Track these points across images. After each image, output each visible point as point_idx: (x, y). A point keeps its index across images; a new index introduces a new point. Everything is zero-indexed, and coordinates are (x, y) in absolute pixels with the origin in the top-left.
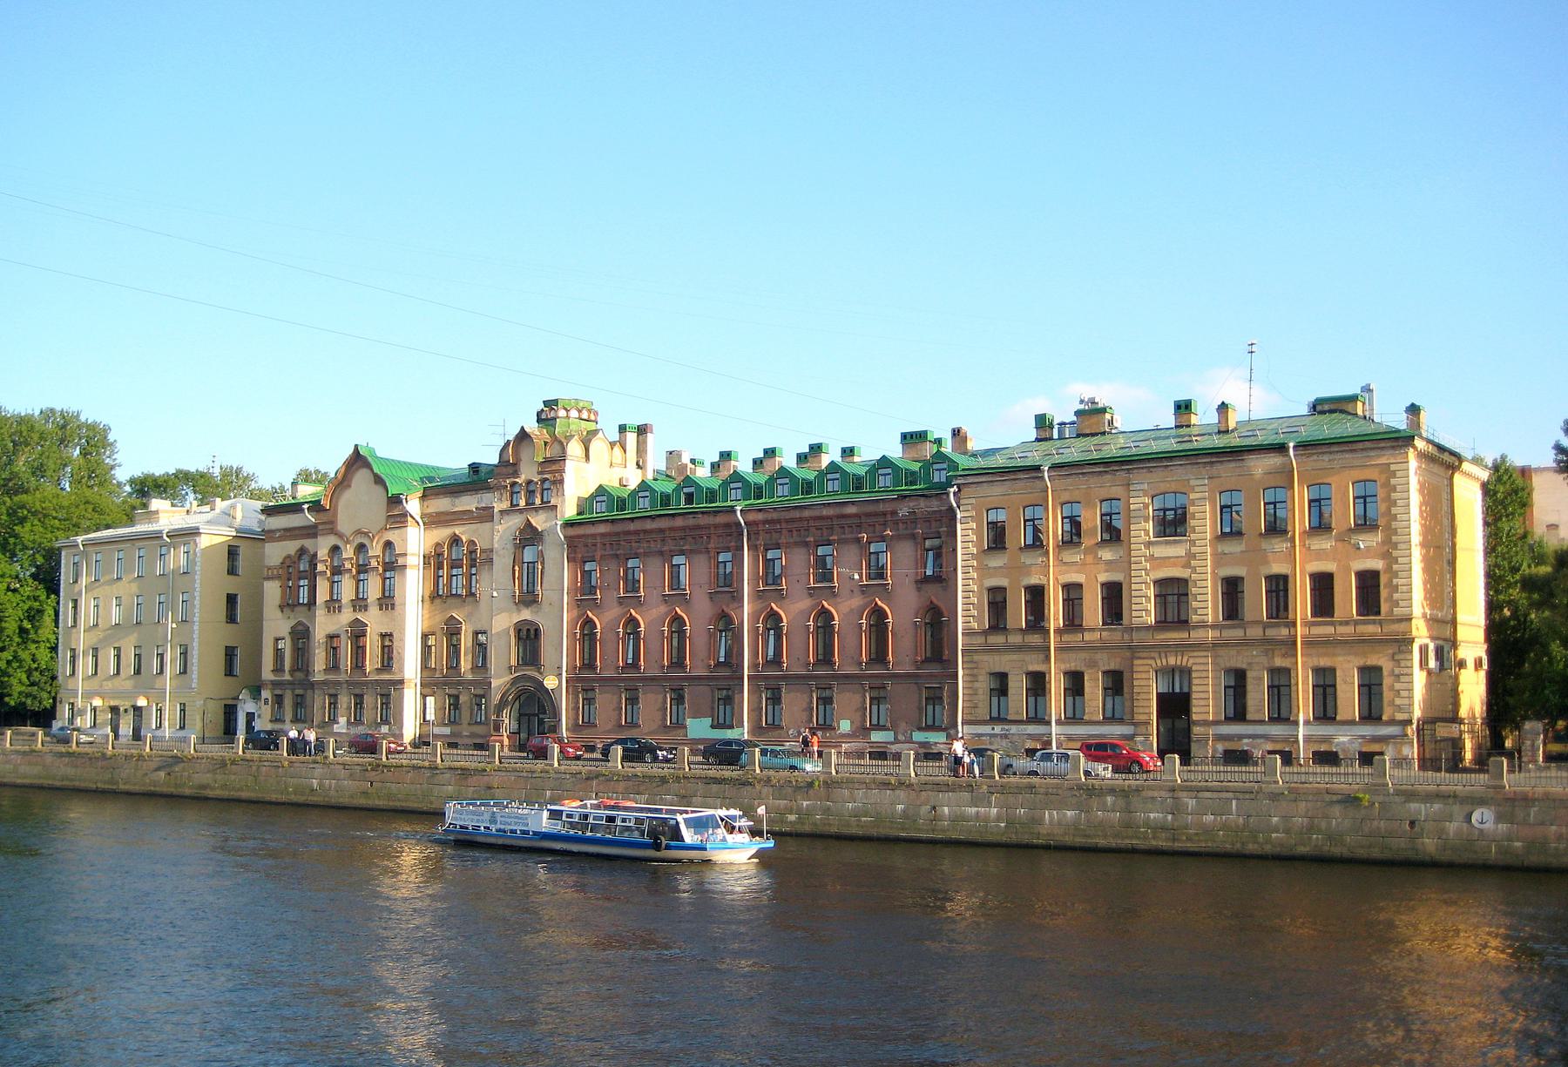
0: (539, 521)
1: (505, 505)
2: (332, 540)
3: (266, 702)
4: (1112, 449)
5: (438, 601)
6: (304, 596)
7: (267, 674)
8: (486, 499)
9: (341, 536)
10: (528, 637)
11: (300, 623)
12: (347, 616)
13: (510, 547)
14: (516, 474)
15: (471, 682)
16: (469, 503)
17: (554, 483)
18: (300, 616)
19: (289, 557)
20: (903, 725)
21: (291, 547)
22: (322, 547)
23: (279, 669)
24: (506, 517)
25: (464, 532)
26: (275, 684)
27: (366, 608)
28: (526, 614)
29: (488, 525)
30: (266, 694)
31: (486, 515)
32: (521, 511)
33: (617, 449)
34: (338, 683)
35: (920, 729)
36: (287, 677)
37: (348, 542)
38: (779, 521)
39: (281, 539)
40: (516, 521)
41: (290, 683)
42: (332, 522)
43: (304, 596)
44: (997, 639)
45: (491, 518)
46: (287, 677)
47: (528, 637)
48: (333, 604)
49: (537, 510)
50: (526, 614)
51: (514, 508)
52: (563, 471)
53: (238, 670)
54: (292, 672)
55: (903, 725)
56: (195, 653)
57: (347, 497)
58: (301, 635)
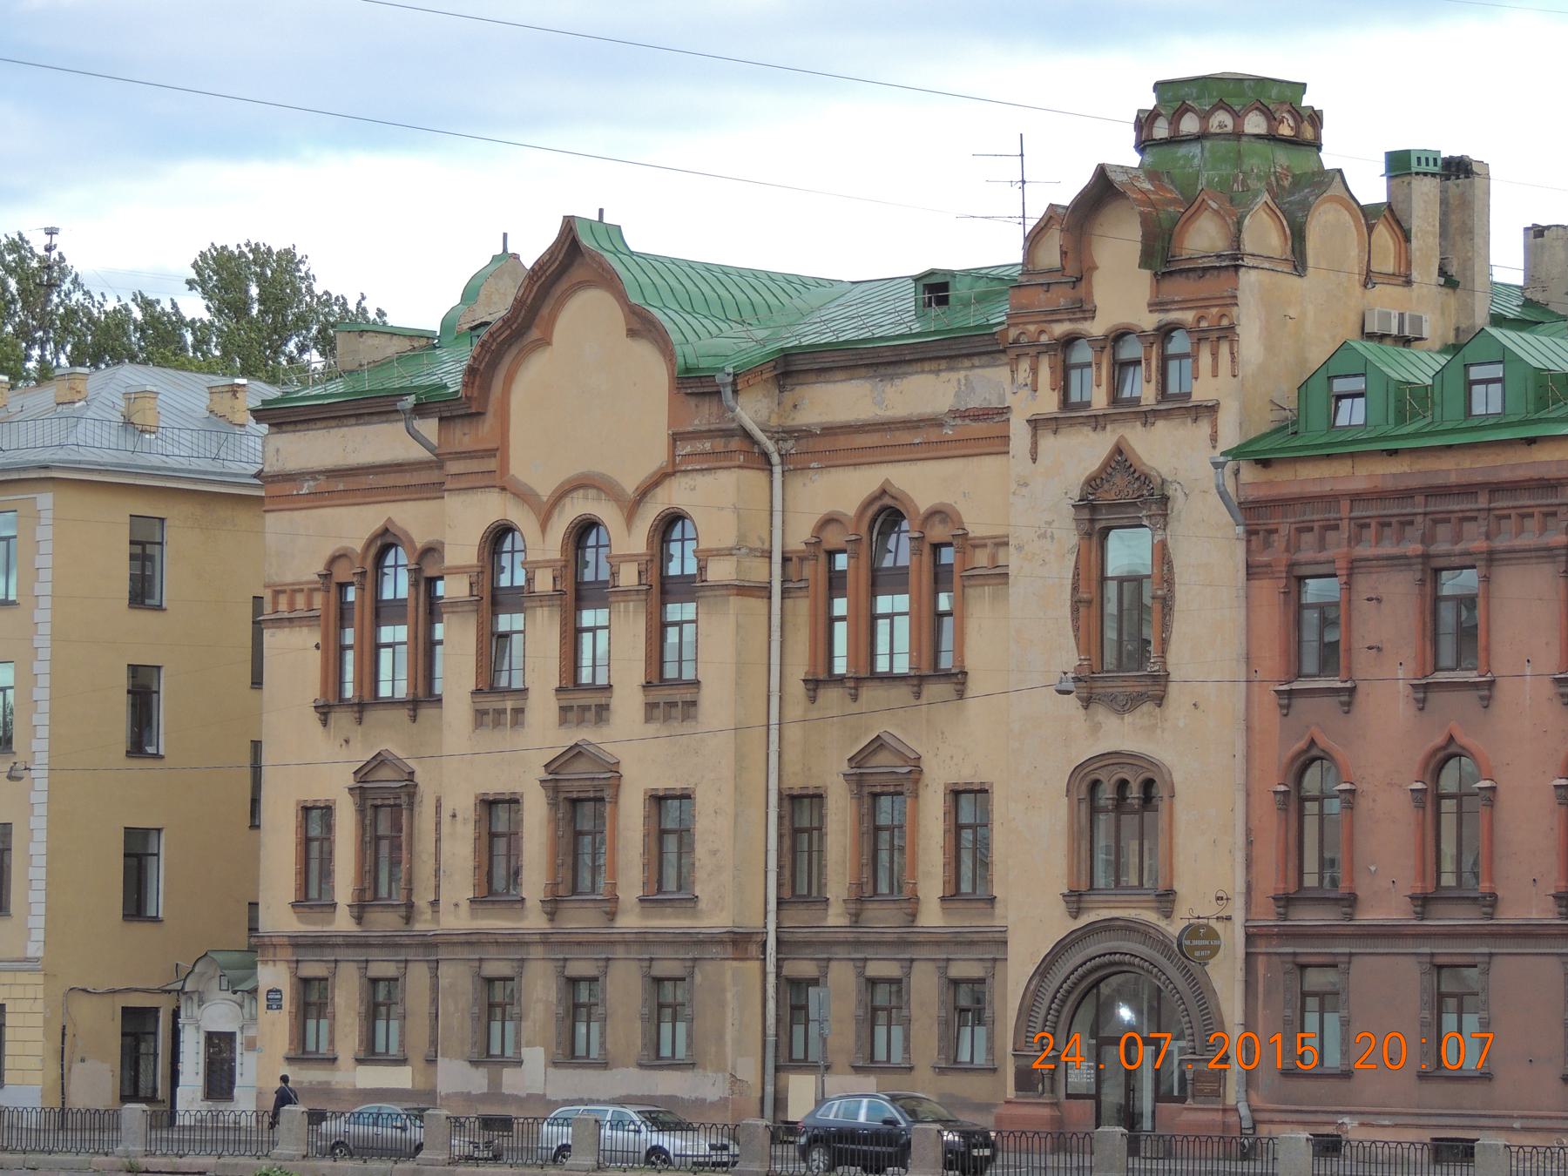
0: (1166, 450)
3: (274, 1001)
5: (832, 697)
6: (393, 679)
7: (278, 917)
8: (990, 383)
9: (523, 495)
10: (1122, 800)
11: (380, 760)
12: (543, 733)
13: (1068, 536)
14: (1083, 309)
15: (938, 941)
16: (926, 393)
17: (1200, 336)
18: (387, 736)
21: (353, 526)
22: (458, 524)
23: (312, 891)
24: (1048, 442)
25: (922, 484)
26: (300, 945)
28: (1120, 734)
29: (990, 464)
30: (273, 975)
31: (982, 431)
32: (1098, 422)
33: (1384, 235)
36: (343, 922)
39: (319, 499)
40: (1084, 453)
41: (351, 943)
42: (498, 452)
43: (393, 679)
45: (1000, 444)
46: (343, 922)
47: (1122, 800)
48: (496, 699)
49: (1147, 417)
50: (1120, 734)
51: (1071, 414)
52: (1233, 301)
53: (159, 899)
56: (39, 848)
57: (533, 386)
58: (386, 802)
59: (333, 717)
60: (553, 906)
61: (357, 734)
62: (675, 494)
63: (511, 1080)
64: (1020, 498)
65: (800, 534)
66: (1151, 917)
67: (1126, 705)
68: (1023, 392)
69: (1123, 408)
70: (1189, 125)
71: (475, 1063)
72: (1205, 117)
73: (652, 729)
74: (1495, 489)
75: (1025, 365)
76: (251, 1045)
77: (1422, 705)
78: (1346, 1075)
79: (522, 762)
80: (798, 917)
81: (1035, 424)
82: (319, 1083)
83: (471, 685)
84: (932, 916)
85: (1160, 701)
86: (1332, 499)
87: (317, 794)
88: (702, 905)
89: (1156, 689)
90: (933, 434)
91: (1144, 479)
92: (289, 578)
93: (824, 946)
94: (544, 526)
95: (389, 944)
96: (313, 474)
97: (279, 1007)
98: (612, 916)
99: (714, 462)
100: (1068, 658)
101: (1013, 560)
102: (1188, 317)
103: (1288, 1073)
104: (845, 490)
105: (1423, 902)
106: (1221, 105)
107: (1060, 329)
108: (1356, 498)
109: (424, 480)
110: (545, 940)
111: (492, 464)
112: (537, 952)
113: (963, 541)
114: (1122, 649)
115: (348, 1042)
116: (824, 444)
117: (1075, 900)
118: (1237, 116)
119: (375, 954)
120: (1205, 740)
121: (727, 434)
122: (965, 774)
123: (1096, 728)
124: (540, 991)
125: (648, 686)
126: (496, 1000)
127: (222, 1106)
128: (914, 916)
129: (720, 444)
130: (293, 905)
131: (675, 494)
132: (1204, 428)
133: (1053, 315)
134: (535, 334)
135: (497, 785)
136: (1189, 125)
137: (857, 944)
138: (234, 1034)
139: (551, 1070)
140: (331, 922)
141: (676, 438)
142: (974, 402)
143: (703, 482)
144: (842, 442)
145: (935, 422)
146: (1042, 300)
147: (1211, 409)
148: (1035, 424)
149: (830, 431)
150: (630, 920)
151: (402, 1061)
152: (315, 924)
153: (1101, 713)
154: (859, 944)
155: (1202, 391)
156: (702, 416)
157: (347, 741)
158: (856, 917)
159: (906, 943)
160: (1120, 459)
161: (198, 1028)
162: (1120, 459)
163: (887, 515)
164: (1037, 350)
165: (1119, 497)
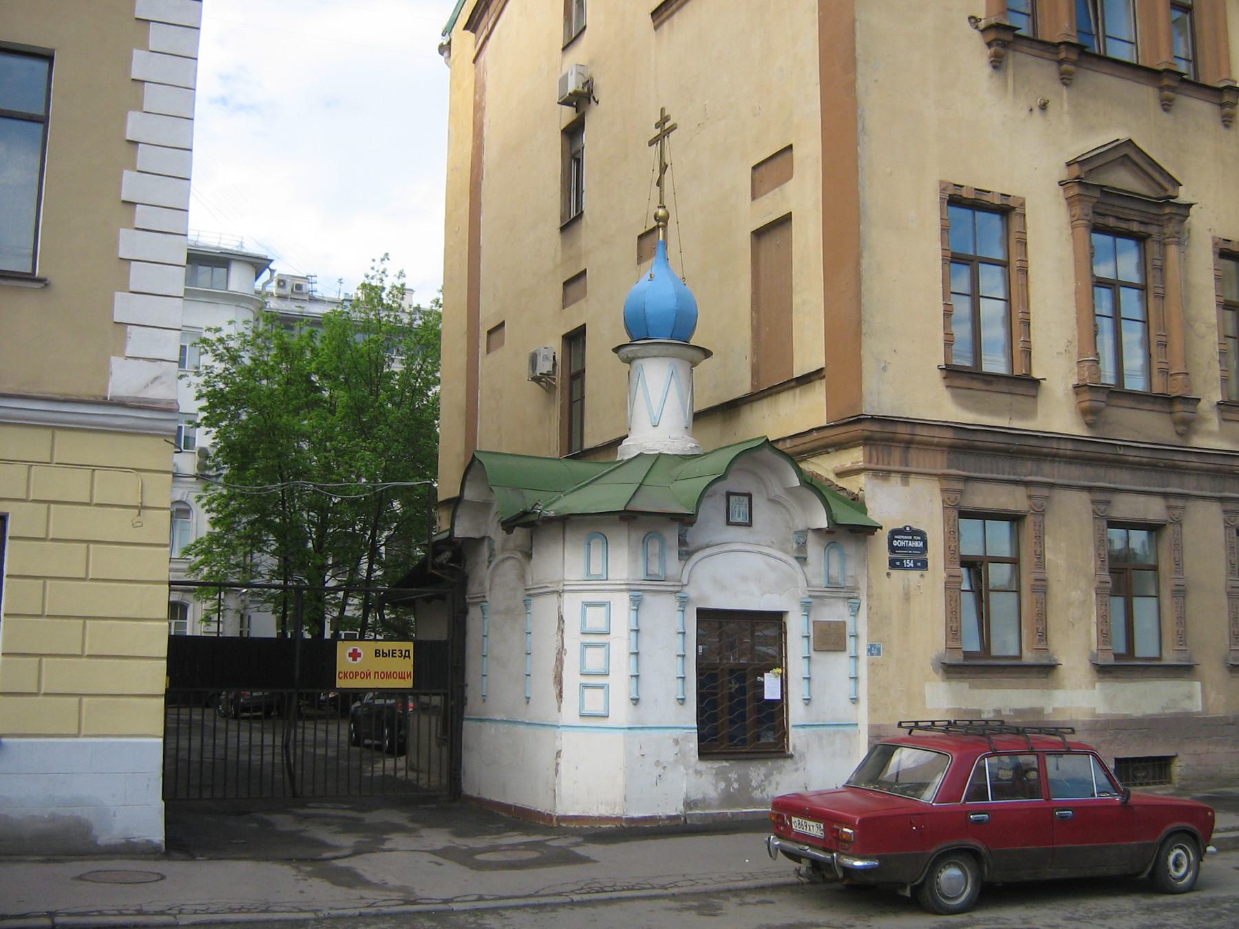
3: (907, 550)
26: (966, 446)
61: (1062, 99)
76: (830, 639)
82: (1019, 712)
87: (995, 180)
97: (924, 565)
115: (1075, 637)
119: (1122, 478)
127: (756, 772)
138: (776, 619)
140: (1030, 414)
151: (1184, 670)
152: (993, 412)
157: (1044, 107)
161: (684, 602)
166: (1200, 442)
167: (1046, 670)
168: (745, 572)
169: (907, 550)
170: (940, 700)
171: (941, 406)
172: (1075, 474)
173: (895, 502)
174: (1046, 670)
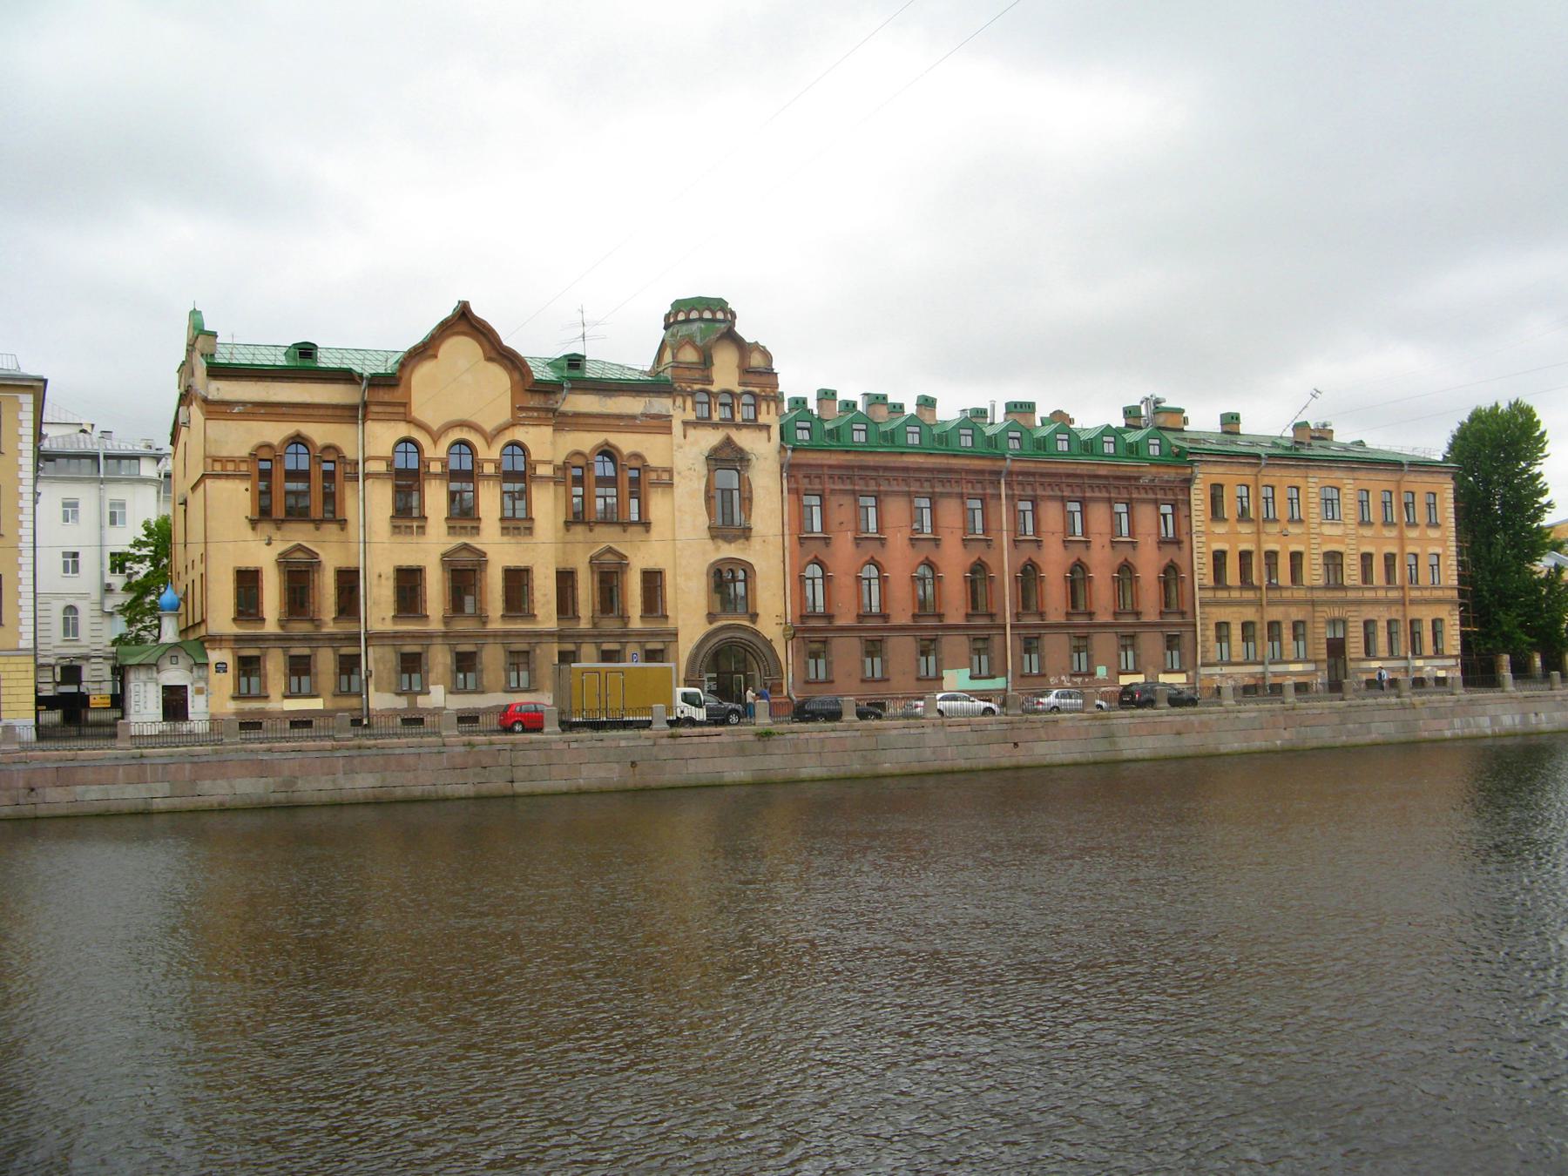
0: (744, 439)
1: (691, 416)
2: (403, 430)
3: (221, 667)
4: (1333, 451)
8: (661, 405)
13: (702, 469)
15: (639, 634)
17: (766, 398)
19: (269, 446)
20: (1151, 670)
21: (275, 432)
22: (382, 437)
24: (691, 432)
25: (626, 443)
26: (238, 639)
27: (476, 530)
28: (729, 551)
31: (661, 424)
32: (716, 426)
34: (429, 636)
35: (1165, 672)
37: (435, 438)
38: (1033, 474)
40: (710, 439)
41: (277, 638)
42: (406, 405)
44: (1222, 594)
45: (668, 430)
49: (738, 427)
50: (729, 551)
51: (703, 422)
54: (282, 623)
55: (1151, 670)
57: (422, 374)
59: (260, 526)
60: (447, 620)
61: (277, 536)
62: (519, 434)
63: (422, 701)
64: (683, 453)
65: (559, 461)
66: (747, 623)
67: (730, 539)
68: (679, 411)
69: (729, 423)
70: (694, 315)
71: (398, 694)
72: (701, 313)
73: (506, 539)
74: (886, 469)
75: (679, 401)
76: (199, 691)
77: (858, 545)
78: (884, 680)
79: (430, 549)
80: (567, 625)
81: (686, 423)
83: (390, 512)
84: (636, 623)
85: (747, 538)
86: (822, 466)
87: (249, 563)
88: (539, 618)
89: (745, 533)
90: (631, 422)
91: (741, 450)
92: (224, 453)
93: (579, 637)
94: (435, 442)
95: (306, 639)
96: (244, 404)
98: (485, 623)
99: (538, 423)
100: (703, 520)
101: (676, 479)
102: (757, 390)
103: (807, 682)
104: (587, 441)
105: (860, 617)
106: (709, 309)
107: (697, 387)
108: (830, 467)
109: (351, 414)
110: (446, 635)
111: (402, 410)
112: (440, 640)
113: (644, 468)
114: (728, 518)
116: (574, 420)
117: (711, 617)
118: (714, 313)
119: (291, 644)
120: (767, 553)
121: (547, 410)
122: (651, 565)
123: (718, 549)
124: (440, 659)
125: (502, 519)
126: (411, 664)
128: (626, 624)
129: (543, 415)
130: (234, 620)
131: (519, 434)
132: (764, 434)
133: (695, 381)
134: (431, 352)
135: (409, 561)
136: (694, 315)
137: (600, 636)
139: (449, 697)
141: (517, 408)
142: (653, 411)
143: (532, 430)
144: (581, 420)
145: (633, 417)
146: (688, 374)
147: (768, 427)
148: (686, 423)
149: (577, 415)
150: (496, 624)
153: (720, 542)
154: (596, 636)
155: (762, 419)
156: (535, 401)
158: (595, 625)
159: (625, 635)
160: (728, 442)
162: (728, 442)
163: (608, 452)
164: (684, 394)
165: (727, 458)
166: (325, 630)
167: (267, 697)
168: (174, 675)
169: (221, 667)
170: (232, 706)
171: (234, 630)
172: (278, 644)
173: (215, 656)
174: (267, 697)
